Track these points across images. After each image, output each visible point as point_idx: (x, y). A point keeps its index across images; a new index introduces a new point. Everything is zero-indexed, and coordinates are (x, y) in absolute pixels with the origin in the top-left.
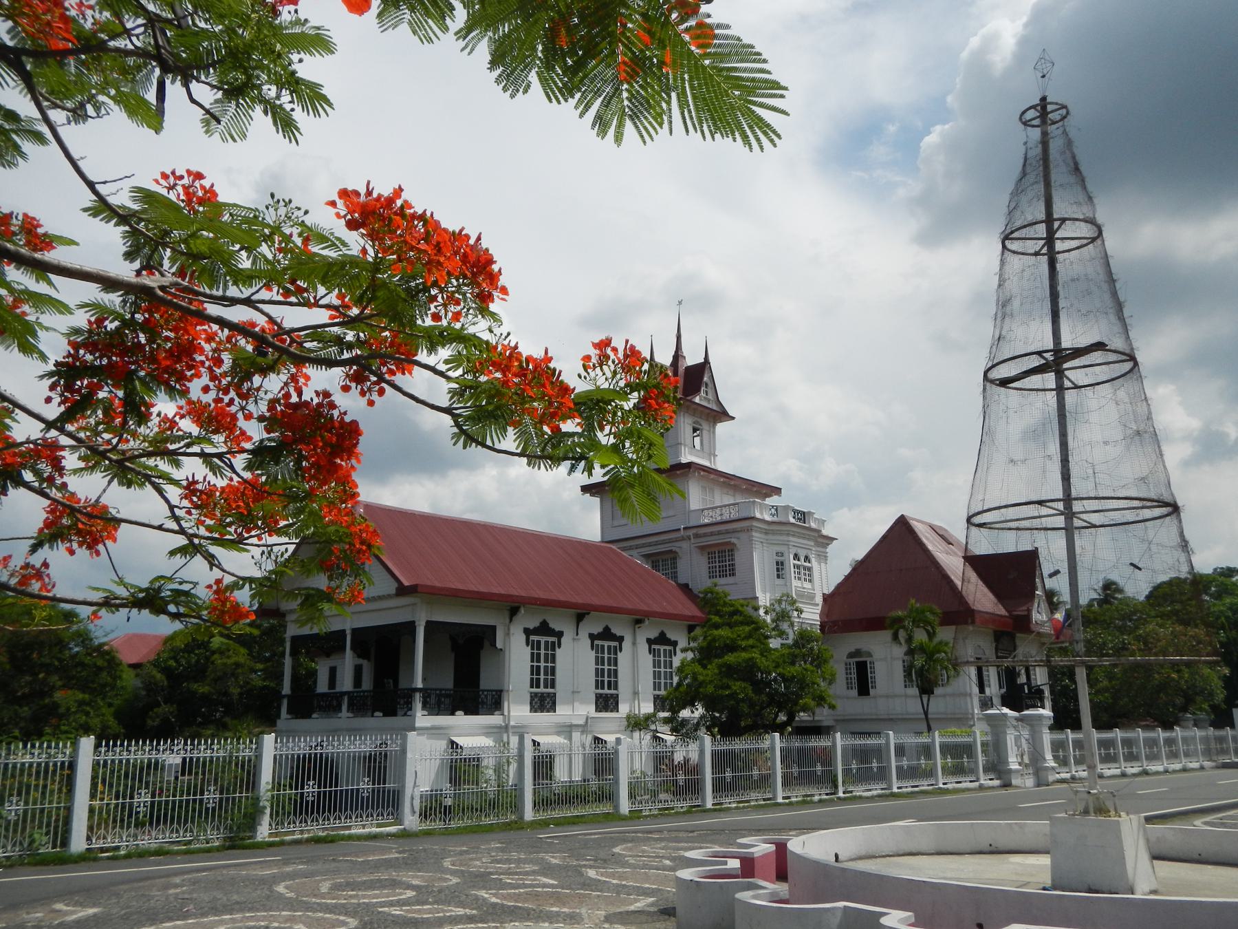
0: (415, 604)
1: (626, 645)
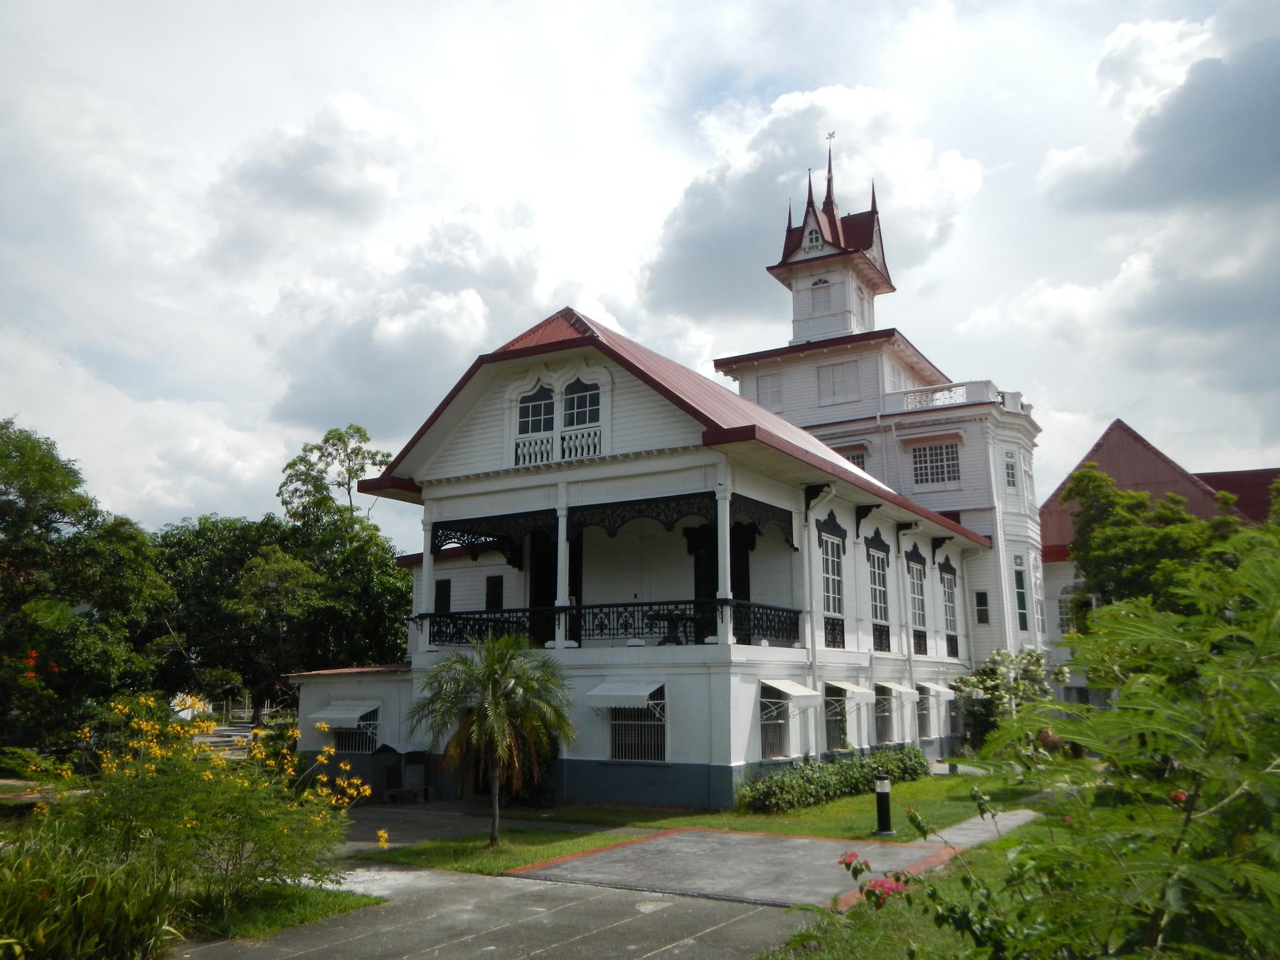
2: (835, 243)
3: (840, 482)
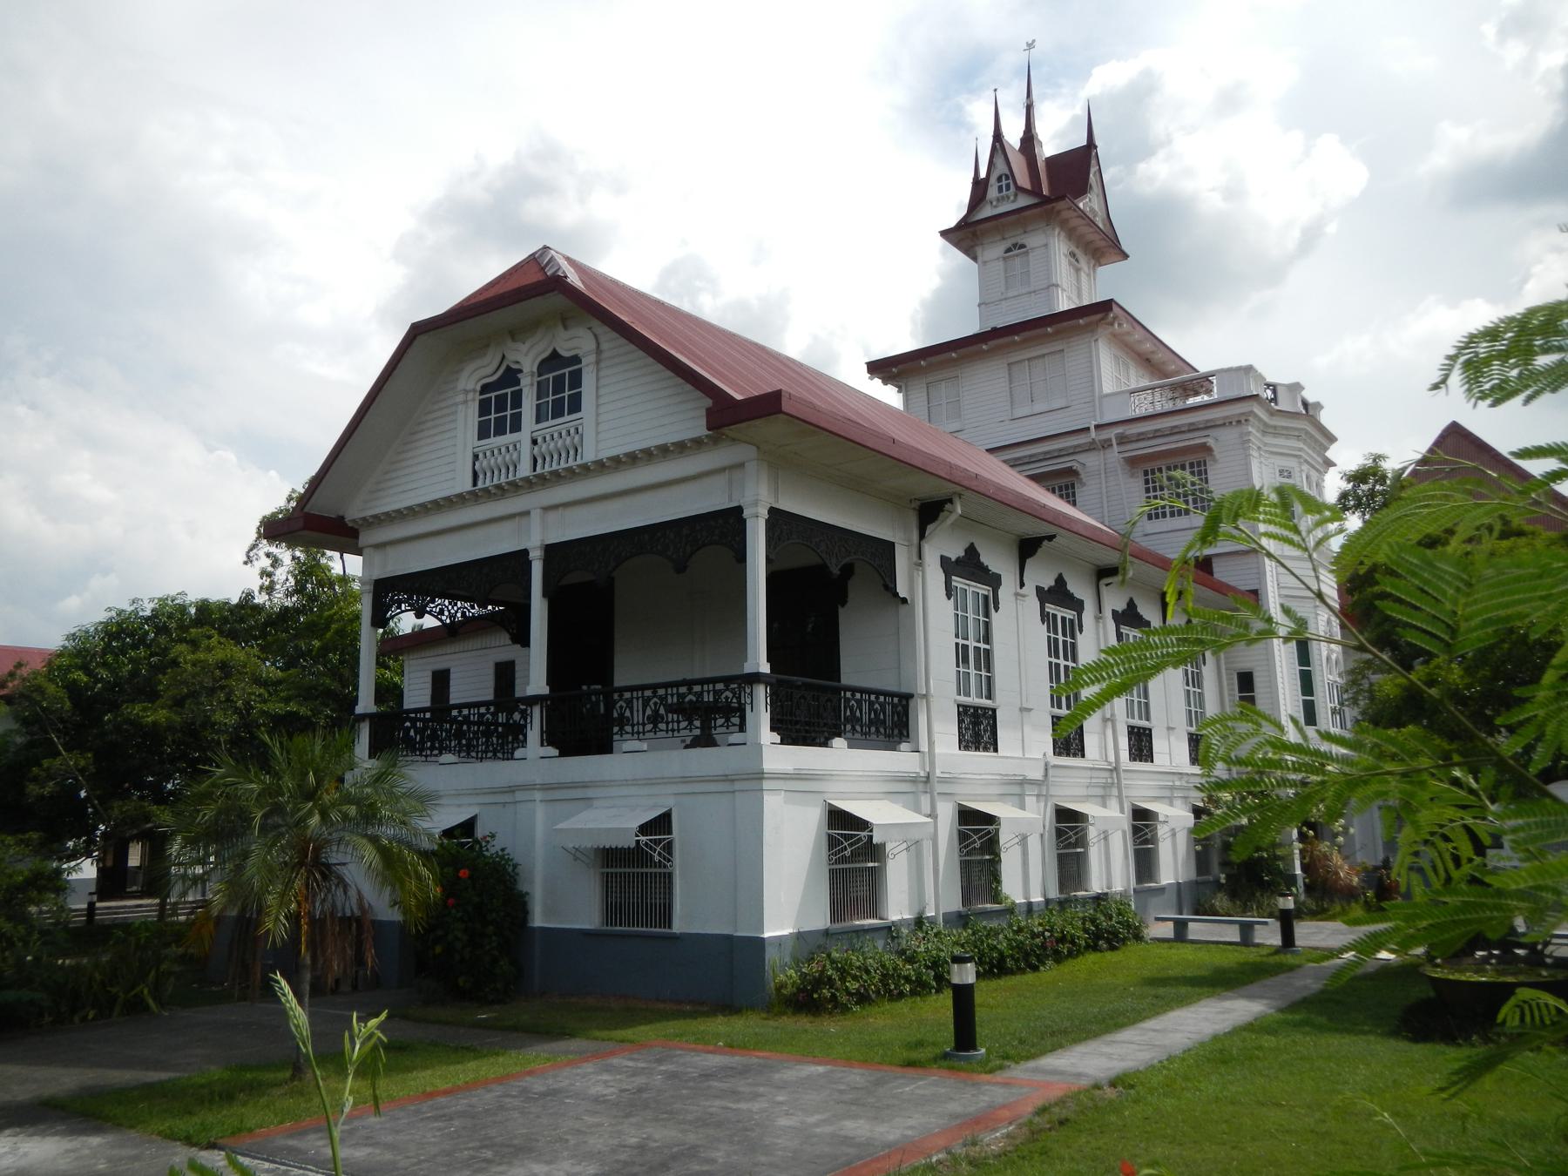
0: (741, 465)
1: (1088, 616)
2: (1035, 191)
3: (967, 494)
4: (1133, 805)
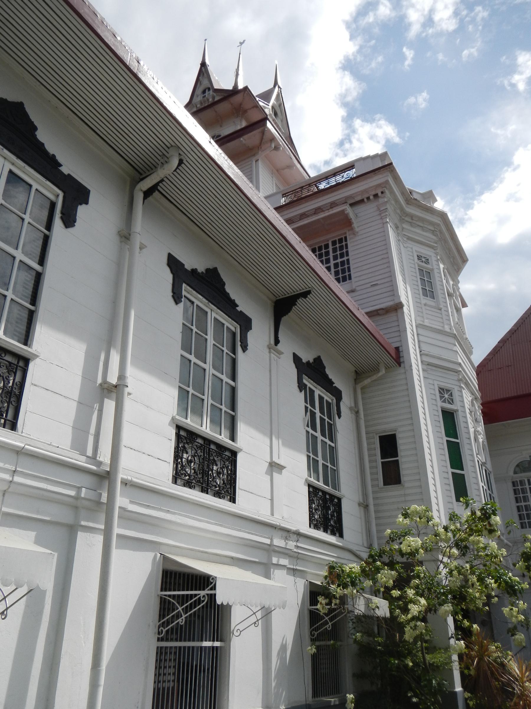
4: (165, 559)
